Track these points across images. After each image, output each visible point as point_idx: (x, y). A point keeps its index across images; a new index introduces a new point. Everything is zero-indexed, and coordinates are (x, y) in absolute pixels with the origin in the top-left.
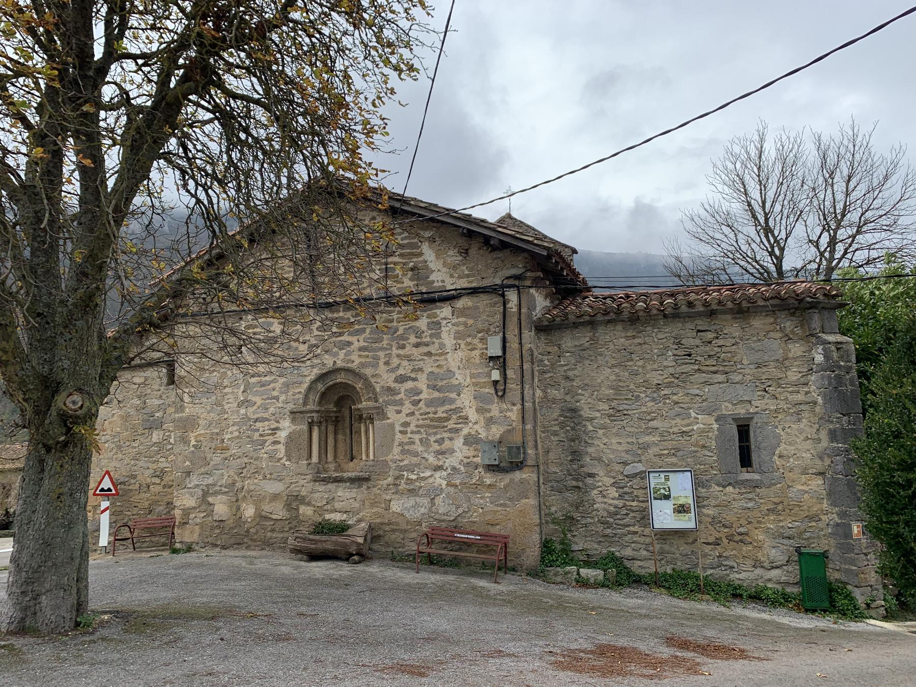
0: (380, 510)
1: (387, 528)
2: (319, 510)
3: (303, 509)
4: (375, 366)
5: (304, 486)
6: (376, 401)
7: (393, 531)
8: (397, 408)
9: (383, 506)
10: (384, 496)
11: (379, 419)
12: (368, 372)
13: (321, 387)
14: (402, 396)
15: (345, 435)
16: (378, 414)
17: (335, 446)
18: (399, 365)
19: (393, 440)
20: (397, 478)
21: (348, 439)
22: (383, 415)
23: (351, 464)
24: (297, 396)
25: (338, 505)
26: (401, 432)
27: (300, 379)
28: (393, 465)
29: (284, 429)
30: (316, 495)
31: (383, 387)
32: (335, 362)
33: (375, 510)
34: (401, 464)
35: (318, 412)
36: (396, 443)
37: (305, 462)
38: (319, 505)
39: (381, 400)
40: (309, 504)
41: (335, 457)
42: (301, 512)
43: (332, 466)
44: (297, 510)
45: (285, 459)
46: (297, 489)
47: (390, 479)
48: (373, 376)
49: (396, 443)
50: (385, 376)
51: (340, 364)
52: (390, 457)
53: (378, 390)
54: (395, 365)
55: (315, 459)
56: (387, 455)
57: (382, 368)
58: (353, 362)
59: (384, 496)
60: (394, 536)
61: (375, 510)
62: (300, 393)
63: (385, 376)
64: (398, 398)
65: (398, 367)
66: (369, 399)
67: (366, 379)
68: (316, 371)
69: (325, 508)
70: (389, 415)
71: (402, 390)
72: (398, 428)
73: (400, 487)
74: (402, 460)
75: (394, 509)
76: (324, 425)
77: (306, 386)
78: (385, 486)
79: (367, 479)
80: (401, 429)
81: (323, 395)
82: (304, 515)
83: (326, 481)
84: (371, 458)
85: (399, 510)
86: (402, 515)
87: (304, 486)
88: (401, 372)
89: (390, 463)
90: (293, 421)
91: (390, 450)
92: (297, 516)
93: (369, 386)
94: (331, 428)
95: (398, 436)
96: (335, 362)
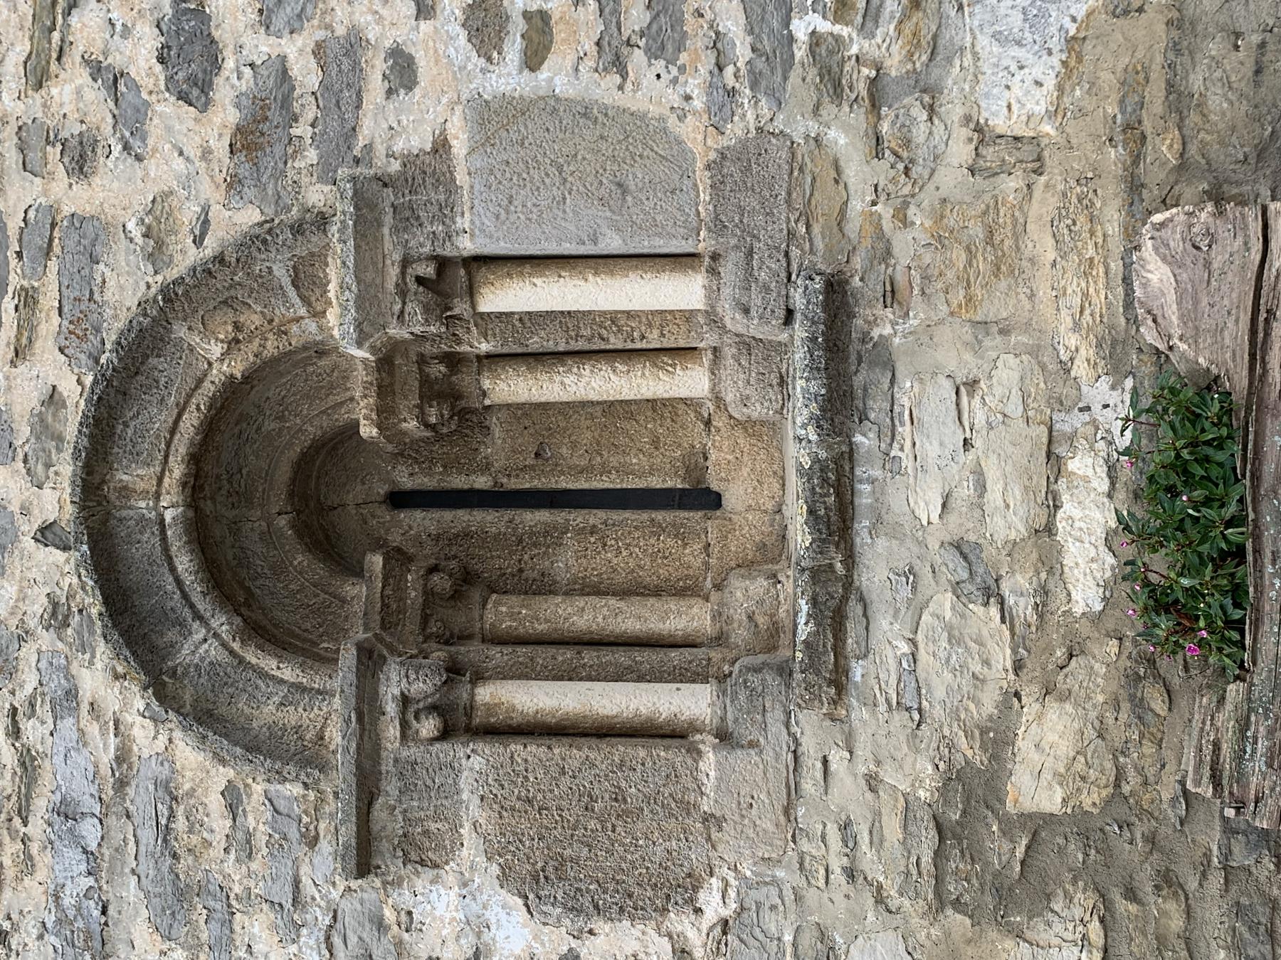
0: (1043, 206)
1: (1165, 149)
2: (1044, 653)
3: (1034, 787)
4: (88, 238)
5: (872, 768)
6: (322, 221)
7: (1179, 101)
8: (375, 86)
9: (1011, 184)
10: (951, 178)
11: (446, 211)
12: (126, 287)
13: (206, 641)
14: (297, 52)
15: (552, 536)
16: (407, 218)
17: (626, 592)
18: (96, 69)
19: (586, 112)
20: (832, 82)
21: (578, 518)
22: (419, 183)
23: (736, 496)
24: (257, 819)
25: (1007, 519)
26: (533, 59)
27: (141, 797)
28: (750, 113)
29: (478, 926)
30: (940, 684)
31: (234, 184)
32: (46, 534)
33: (1042, 245)
34: (742, 52)
35: (370, 661)
36: (604, 89)
37: (710, 762)
38: (1003, 657)
39: (317, 195)
40: (998, 739)
41: (686, 590)
42: (1051, 800)
43: (746, 593)
44: (1037, 826)
45: (680, 922)
46: (892, 829)
47: (838, 138)
48: (157, 253)
49: (604, 89)
50: (164, 170)
51: (56, 501)
52: (695, 136)
53: (249, 217)
54: (95, 95)
55: (691, 702)
56: (679, 156)
57: (114, 192)
58: (53, 398)
59: (951, 178)
60: (1216, 101)
61: (1042, 245)
62: (233, 800)
63: (164, 170)
64: (306, 75)
65: (113, 80)
66: (307, 279)
67: (172, 302)
68: (99, 675)
69: (1023, 608)
70: (418, 140)
71: (262, 47)
72: (506, 77)
73: (895, 65)
74: (718, 44)
75: (1039, 103)
76: (471, 652)
77: (189, 756)
78: (882, 171)
79: (836, 293)
80: (513, 49)
81: (262, 631)
82: (1071, 777)
83: (837, 601)
84: (682, 292)
85: (1047, 69)
86: (1073, 44)
87: (872, 768)
88: (140, 55)
89: (735, 130)
90: (423, 853)
91: (641, 132)
92: (1080, 825)
93: (211, 288)
94: (503, 613)
95: (558, 76)
96: (46, 534)
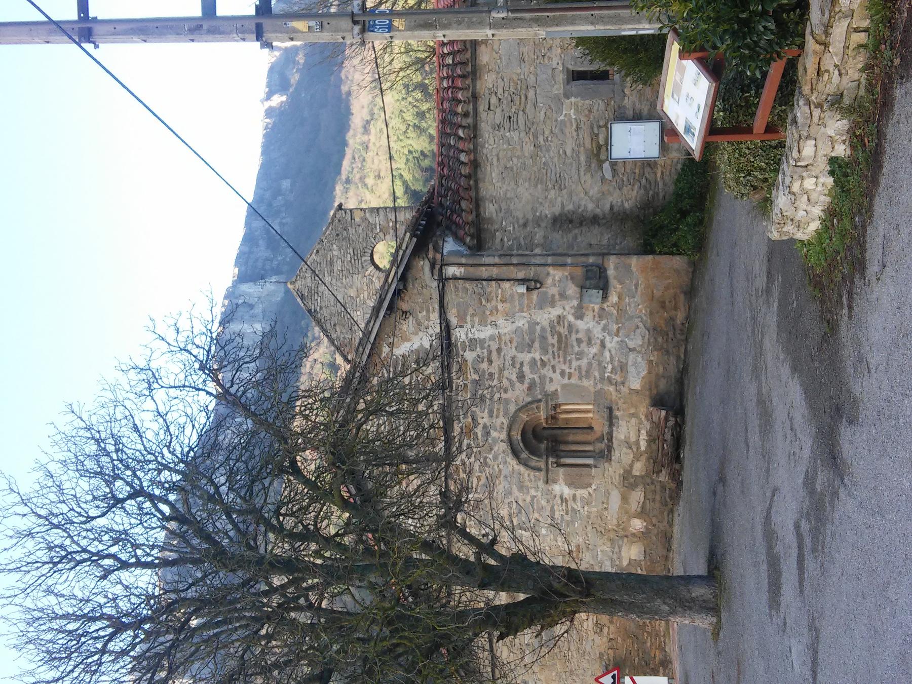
4: (507, 401)
6: (540, 401)
12: (512, 408)
13: (524, 455)
19: (577, 386)
24: (532, 477)
26: (569, 379)
28: (599, 386)
29: (562, 490)
32: (502, 441)
35: (547, 457)
39: (540, 397)
40: (631, 466)
41: (588, 443)
42: (638, 474)
44: (636, 476)
45: (589, 489)
46: (617, 477)
49: (579, 382)
50: (517, 392)
51: (504, 436)
55: (590, 461)
58: (503, 423)
62: (529, 475)
63: (517, 392)
64: (537, 380)
67: (519, 410)
71: (531, 376)
72: (566, 381)
77: (522, 469)
79: (610, 410)
80: (567, 377)
83: (610, 448)
84: (590, 407)
87: (613, 470)
88: (514, 377)
90: (555, 482)
92: (642, 477)
94: (563, 447)
95: (574, 380)
96: (502, 441)
